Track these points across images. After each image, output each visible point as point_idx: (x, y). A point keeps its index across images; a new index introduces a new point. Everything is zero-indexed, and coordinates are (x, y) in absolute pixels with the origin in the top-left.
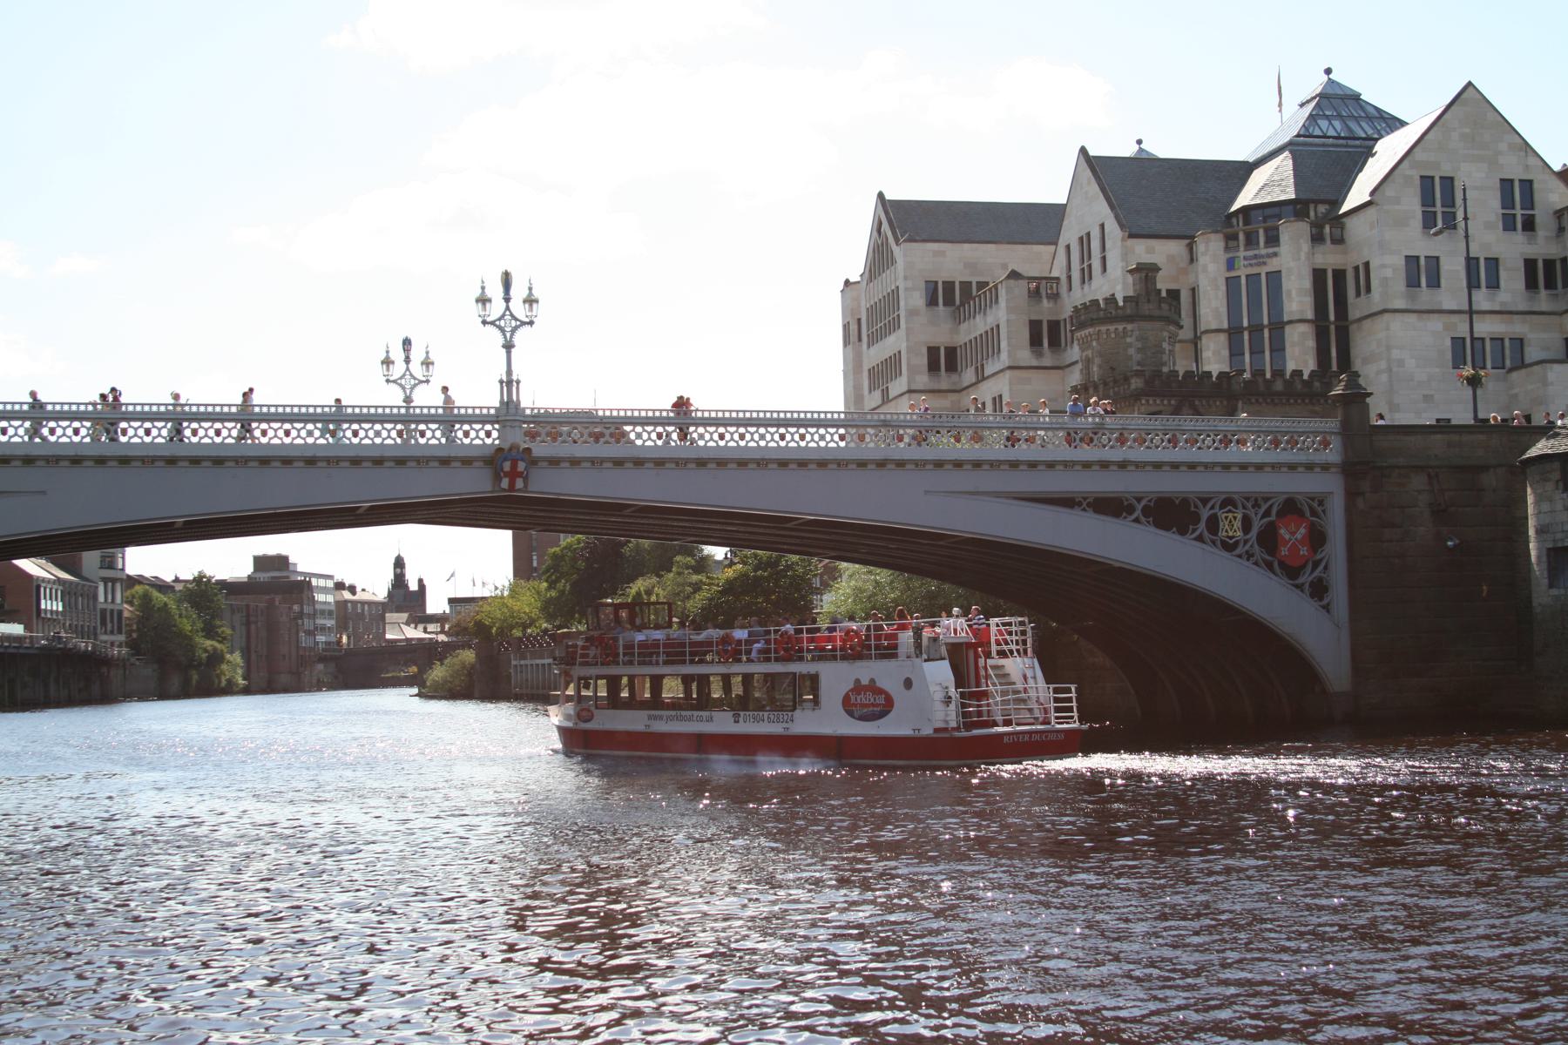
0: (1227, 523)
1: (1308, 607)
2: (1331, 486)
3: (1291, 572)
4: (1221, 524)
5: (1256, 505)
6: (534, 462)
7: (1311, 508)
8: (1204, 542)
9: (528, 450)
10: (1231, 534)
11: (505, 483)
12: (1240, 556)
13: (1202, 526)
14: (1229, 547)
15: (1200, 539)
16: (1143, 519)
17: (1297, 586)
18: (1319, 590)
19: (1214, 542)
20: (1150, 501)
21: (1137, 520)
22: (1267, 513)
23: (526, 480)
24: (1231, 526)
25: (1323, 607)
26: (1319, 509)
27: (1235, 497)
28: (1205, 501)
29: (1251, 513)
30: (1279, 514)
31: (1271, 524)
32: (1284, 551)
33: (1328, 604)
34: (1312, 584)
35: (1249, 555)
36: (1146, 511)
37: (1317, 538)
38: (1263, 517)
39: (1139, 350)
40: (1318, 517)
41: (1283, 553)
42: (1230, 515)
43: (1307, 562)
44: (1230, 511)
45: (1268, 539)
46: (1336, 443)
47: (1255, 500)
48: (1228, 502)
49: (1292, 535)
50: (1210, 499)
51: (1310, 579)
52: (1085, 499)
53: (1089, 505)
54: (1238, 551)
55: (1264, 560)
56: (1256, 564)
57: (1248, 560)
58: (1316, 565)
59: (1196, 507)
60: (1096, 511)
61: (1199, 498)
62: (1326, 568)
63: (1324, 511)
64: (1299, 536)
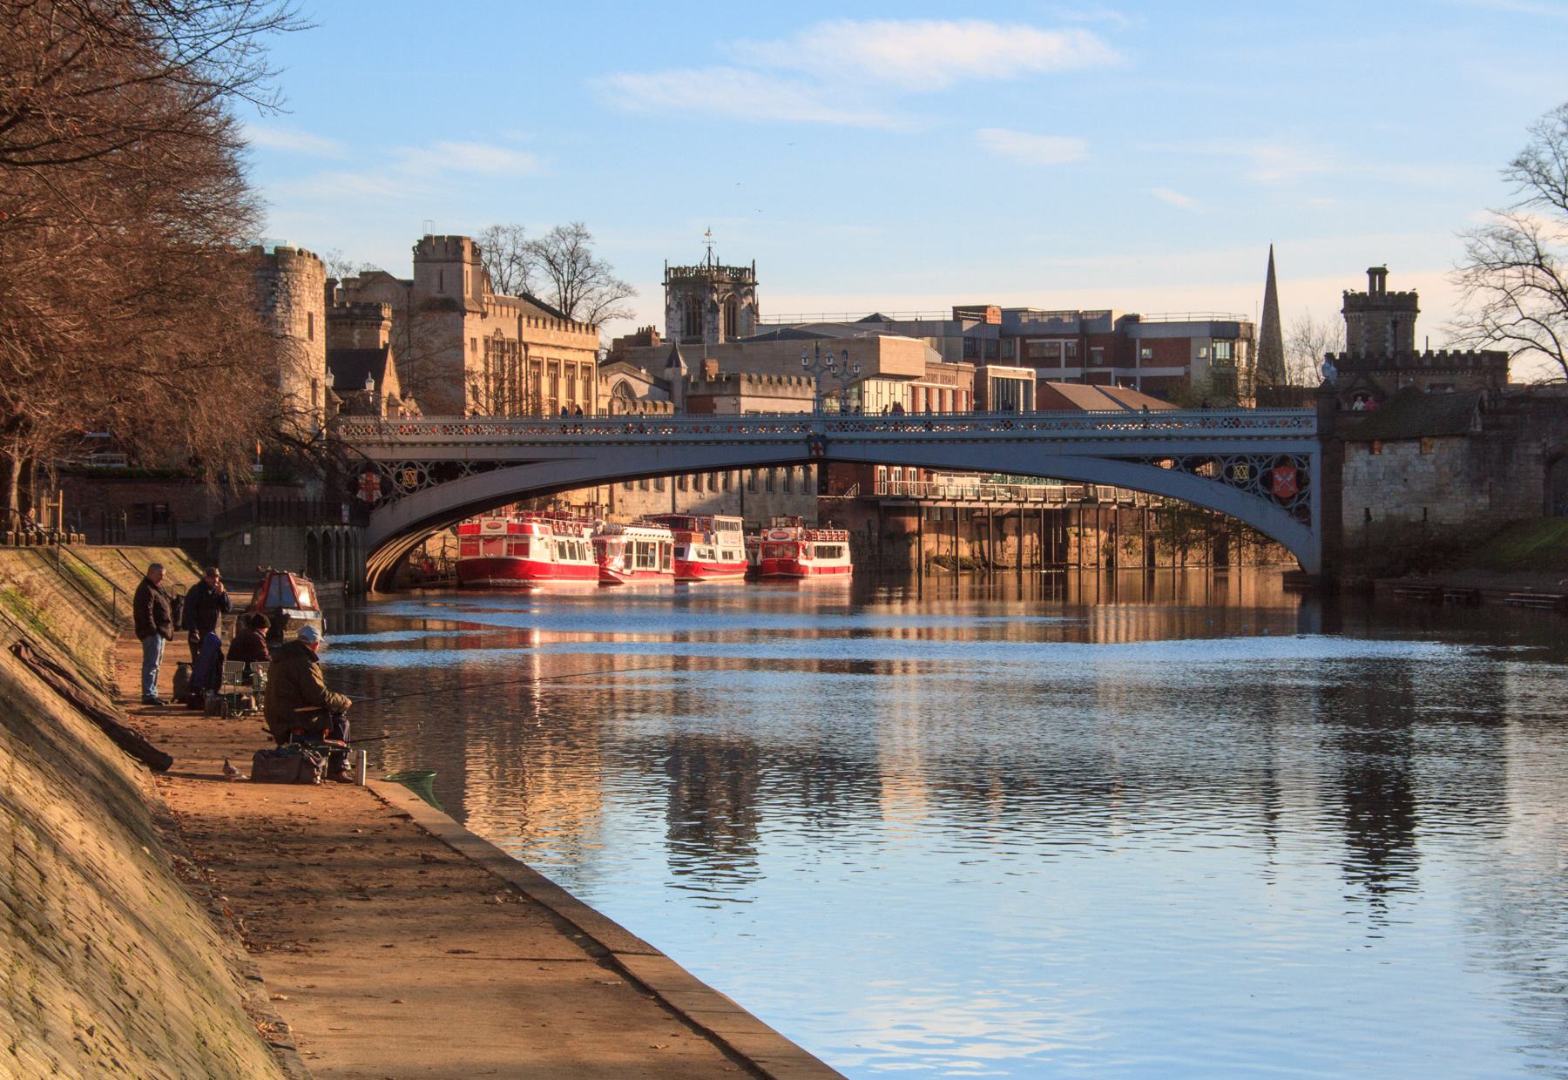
1: (1293, 523)
2: (1314, 449)
3: (1283, 501)
9: (823, 436)
14: (1241, 485)
18: (1302, 513)
22: (1268, 465)
24: (1242, 472)
26: (1305, 463)
29: (1256, 464)
32: (1277, 489)
34: (1298, 509)
35: (1255, 491)
37: (1302, 481)
39: (1368, 331)
46: (1315, 422)
49: (1284, 480)
55: (1266, 495)
58: (1301, 497)
62: (1309, 498)
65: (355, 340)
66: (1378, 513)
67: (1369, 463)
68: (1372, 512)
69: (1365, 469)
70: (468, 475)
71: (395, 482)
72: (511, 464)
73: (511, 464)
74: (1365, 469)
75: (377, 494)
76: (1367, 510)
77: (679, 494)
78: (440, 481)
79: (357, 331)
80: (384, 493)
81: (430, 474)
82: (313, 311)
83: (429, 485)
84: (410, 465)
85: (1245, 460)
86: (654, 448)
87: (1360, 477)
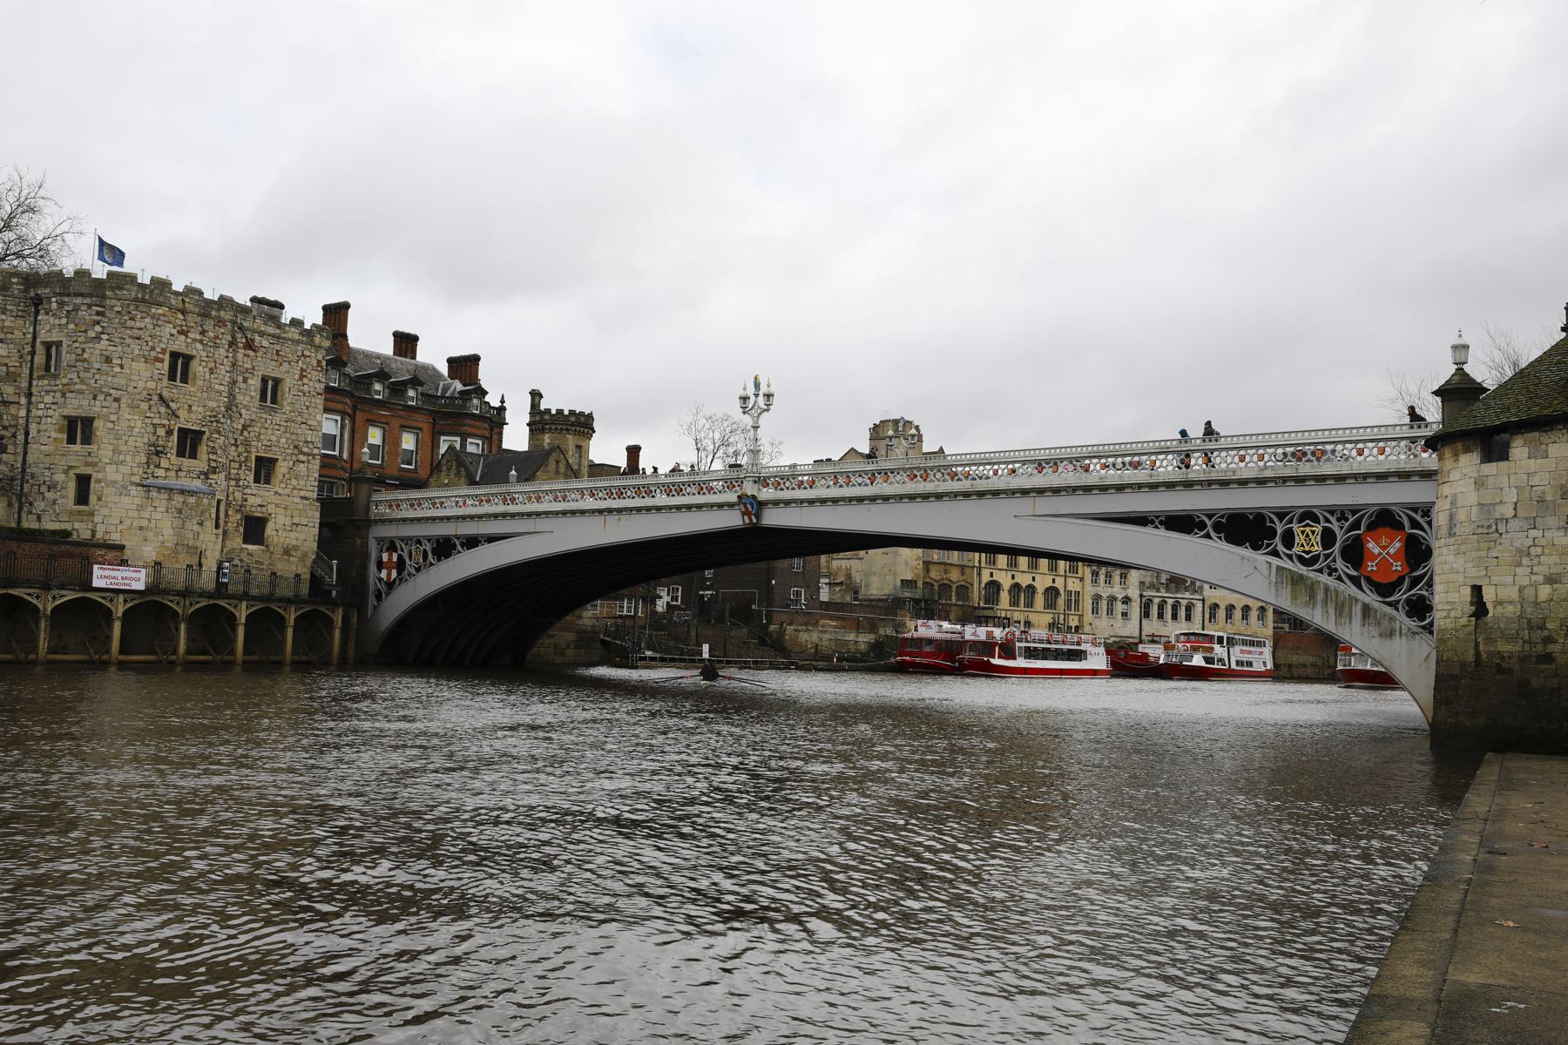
0: (1302, 537)
3: (1384, 590)
4: (1297, 538)
5: (1342, 518)
6: (762, 504)
7: (1412, 520)
8: (1279, 557)
10: (1307, 549)
11: (747, 521)
12: (1320, 571)
13: (1277, 539)
15: (1275, 553)
16: (1213, 534)
17: (1389, 604)
19: (1290, 557)
20: (1222, 517)
21: (1208, 536)
22: (1356, 526)
23: (758, 516)
24: (1308, 539)
25: (1423, 627)
26: (1421, 520)
27: (1314, 510)
28: (1282, 514)
29: (1335, 526)
30: (1371, 527)
31: (1358, 538)
32: (1371, 566)
33: (1431, 624)
34: (1408, 601)
36: (1218, 527)
38: (1350, 529)
40: (1423, 529)
41: (1369, 569)
42: (1308, 529)
43: (1400, 581)
44: (1308, 525)
45: (1355, 553)
47: (1341, 513)
48: (1308, 515)
49: (1384, 550)
50: (1288, 513)
51: (1405, 596)
52: (1157, 517)
53: (1161, 523)
54: (1315, 567)
55: (1350, 577)
56: (1339, 578)
57: (1330, 575)
58: (1415, 582)
59: (1272, 521)
60: (1168, 528)
61: (1277, 514)
62: (1430, 584)
63: (1430, 523)
64: (1392, 551)
65: (545, 445)
66: (1502, 592)
67: (1480, 483)
68: (1488, 595)
69: (1473, 498)
70: (460, 552)
71: (408, 561)
72: (492, 539)
73: (492, 539)
74: (1473, 498)
75: (394, 574)
76: (1477, 590)
77: (1144, 621)
78: (439, 560)
79: (547, 435)
80: (399, 573)
81: (434, 551)
82: (198, 350)
83: (431, 564)
84: (419, 542)
85: (1316, 520)
86: (600, 519)
87: (1461, 515)
